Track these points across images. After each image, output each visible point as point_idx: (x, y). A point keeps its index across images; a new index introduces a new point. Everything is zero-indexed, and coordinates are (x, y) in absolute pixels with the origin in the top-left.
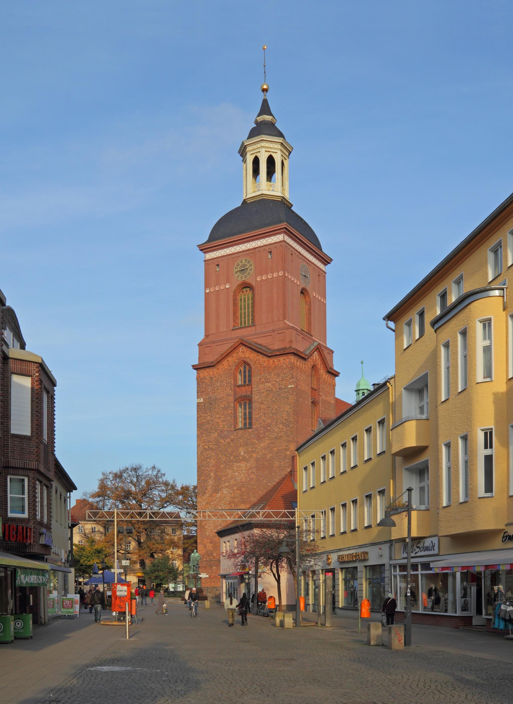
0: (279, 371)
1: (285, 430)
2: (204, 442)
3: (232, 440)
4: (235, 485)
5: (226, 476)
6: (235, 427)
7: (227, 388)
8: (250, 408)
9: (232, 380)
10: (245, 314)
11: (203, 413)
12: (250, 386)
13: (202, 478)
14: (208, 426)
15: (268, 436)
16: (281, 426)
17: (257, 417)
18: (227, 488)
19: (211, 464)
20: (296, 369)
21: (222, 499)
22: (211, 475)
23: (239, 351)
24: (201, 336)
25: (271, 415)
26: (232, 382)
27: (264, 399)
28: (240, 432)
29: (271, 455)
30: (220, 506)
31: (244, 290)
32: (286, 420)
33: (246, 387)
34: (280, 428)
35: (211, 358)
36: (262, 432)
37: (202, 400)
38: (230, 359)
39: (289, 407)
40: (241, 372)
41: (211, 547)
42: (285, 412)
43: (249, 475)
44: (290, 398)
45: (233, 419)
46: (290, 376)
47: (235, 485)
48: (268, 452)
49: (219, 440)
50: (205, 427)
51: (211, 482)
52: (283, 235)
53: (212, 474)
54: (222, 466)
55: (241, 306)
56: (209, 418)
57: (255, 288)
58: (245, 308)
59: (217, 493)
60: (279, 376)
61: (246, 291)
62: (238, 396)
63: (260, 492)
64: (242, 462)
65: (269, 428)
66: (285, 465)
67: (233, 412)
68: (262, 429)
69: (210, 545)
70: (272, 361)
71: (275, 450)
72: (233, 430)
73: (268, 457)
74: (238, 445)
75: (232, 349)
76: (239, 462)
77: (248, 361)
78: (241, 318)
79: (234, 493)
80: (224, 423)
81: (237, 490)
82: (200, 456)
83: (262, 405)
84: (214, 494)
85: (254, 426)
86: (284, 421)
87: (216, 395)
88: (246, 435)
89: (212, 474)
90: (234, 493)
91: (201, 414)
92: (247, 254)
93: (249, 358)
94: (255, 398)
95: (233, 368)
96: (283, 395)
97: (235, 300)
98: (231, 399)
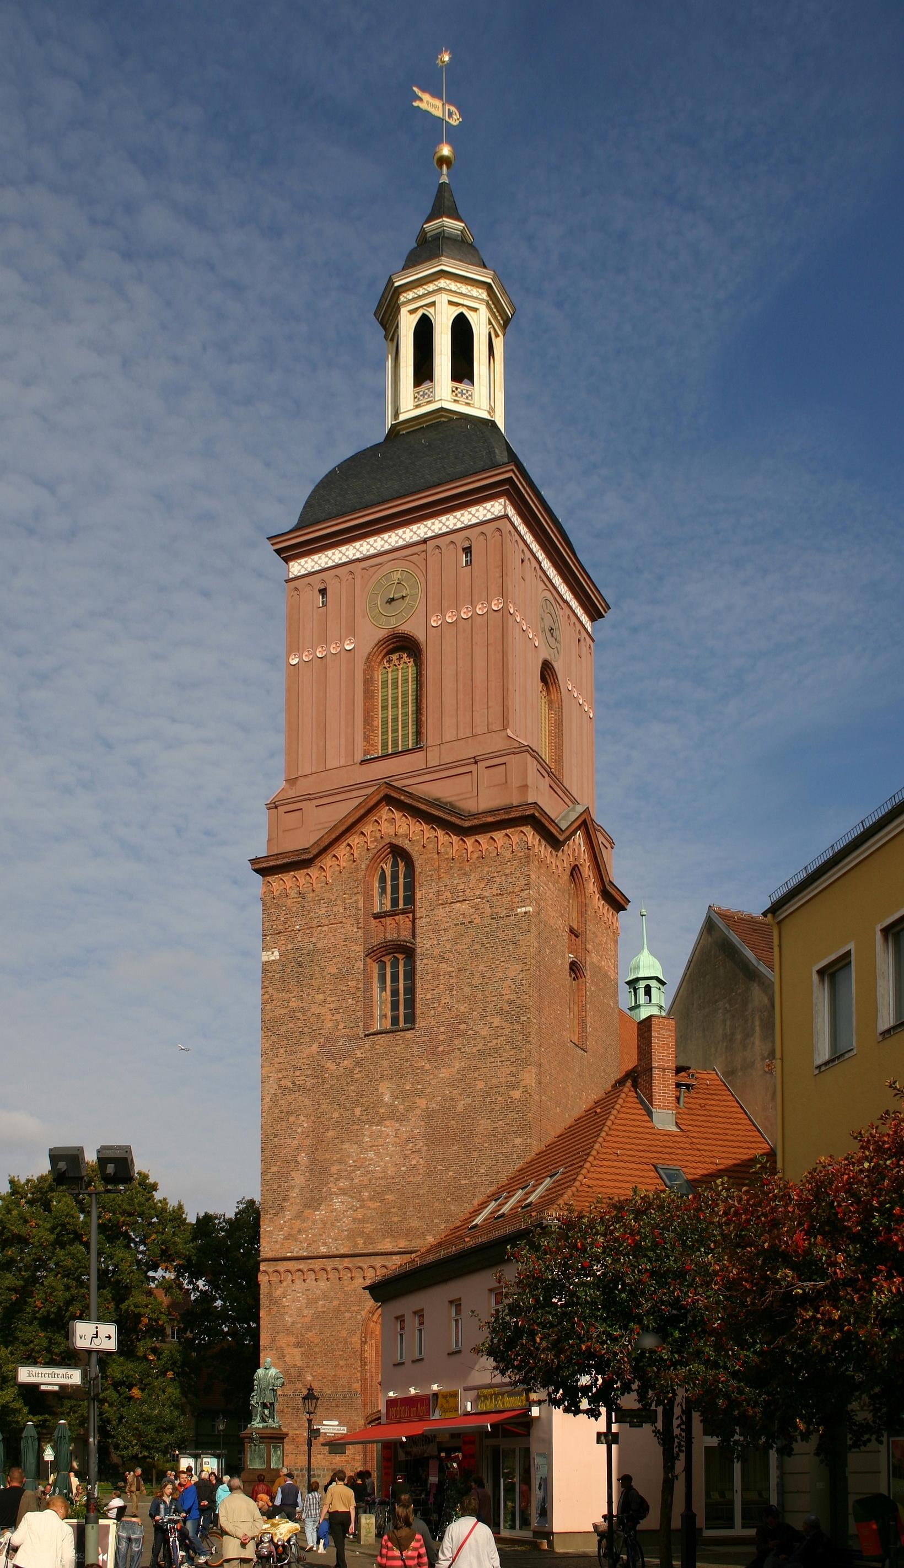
0: (492, 869)
1: (507, 1032)
2: (280, 1070)
3: (358, 1063)
4: (365, 1187)
5: (340, 1161)
6: (367, 1026)
7: (344, 920)
8: (411, 975)
9: (360, 898)
10: (395, 720)
11: (278, 991)
12: (411, 915)
13: (274, 1169)
14: (291, 1025)
15: (460, 1049)
16: (496, 1021)
17: (429, 996)
18: (345, 1194)
19: (299, 1131)
20: (536, 863)
21: (328, 1225)
22: (299, 1159)
23: (380, 818)
25: (467, 990)
26: (361, 905)
27: (449, 947)
28: (382, 1039)
29: (469, 1100)
30: (325, 1244)
31: (394, 657)
32: (510, 1002)
33: (397, 918)
34: (494, 1025)
36: (441, 1037)
38: (355, 840)
39: (519, 967)
40: (383, 879)
41: (298, 1358)
42: (509, 982)
43: (406, 1157)
44: (521, 943)
45: (361, 1005)
46: (524, 882)
47: (365, 1187)
48: (461, 1094)
49: (322, 1063)
50: (283, 1029)
51: (298, 1179)
52: (502, 501)
53: (303, 1158)
54: (331, 1134)
55: (385, 700)
56: (294, 1004)
57: (423, 646)
58: (395, 706)
59: (317, 1209)
60: (490, 880)
61: (400, 658)
62: (375, 942)
63: (437, 1204)
64: (387, 1123)
65: (463, 1027)
66: (506, 1128)
67: (361, 985)
68: (442, 1029)
69: (297, 1351)
70: (473, 840)
71: (478, 1088)
72: (362, 1035)
73: (460, 1107)
74: (377, 1077)
75: (362, 811)
76: (380, 1122)
77: (406, 844)
78: (385, 733)
79: (361, 1207)
80: (337, 1017)
81: (372, 1199)
82: (270, 1108)
83: (444, 965)
84: (308, 1212)
85: (420, 1023)
86: (506, 1007)
87: (314, 940)
88: (398, 1048)
90: (361, 1207)
91: (274, 993)
92: (404, 558)
93: (407, 836)
94: (424, 944)
95: (363, 866)
96: (502, 936)
97: (368, 682)
98: (358, 949)
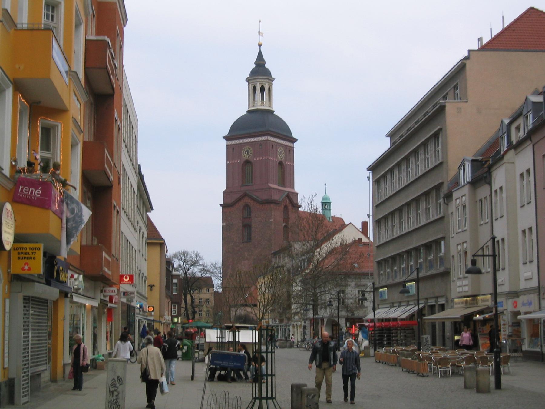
6: (242, 241)
24: (225, 188)
35: (230, 201)
37: (225, 224)
53: (230, 267)
89: (230, 267)
94: (253, 225)
98: (241, 225)
